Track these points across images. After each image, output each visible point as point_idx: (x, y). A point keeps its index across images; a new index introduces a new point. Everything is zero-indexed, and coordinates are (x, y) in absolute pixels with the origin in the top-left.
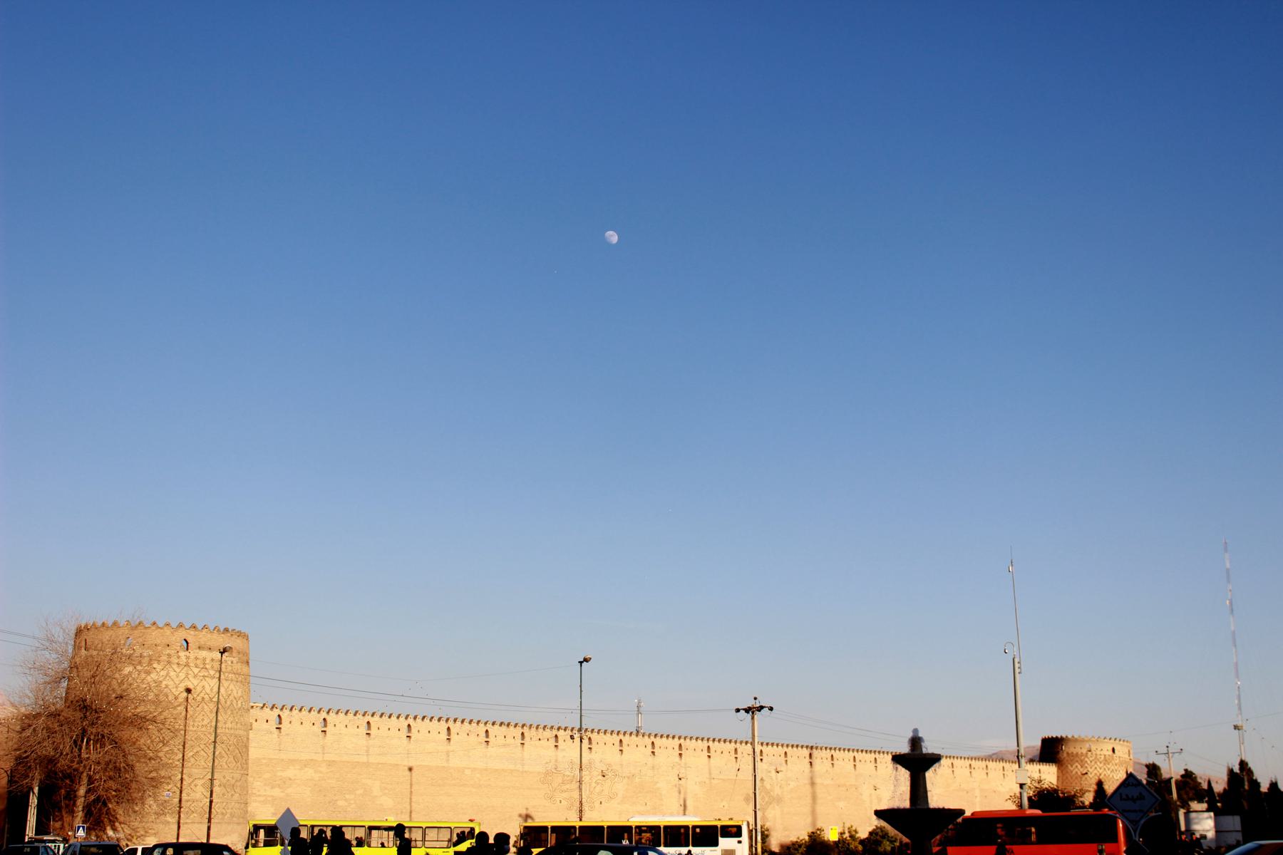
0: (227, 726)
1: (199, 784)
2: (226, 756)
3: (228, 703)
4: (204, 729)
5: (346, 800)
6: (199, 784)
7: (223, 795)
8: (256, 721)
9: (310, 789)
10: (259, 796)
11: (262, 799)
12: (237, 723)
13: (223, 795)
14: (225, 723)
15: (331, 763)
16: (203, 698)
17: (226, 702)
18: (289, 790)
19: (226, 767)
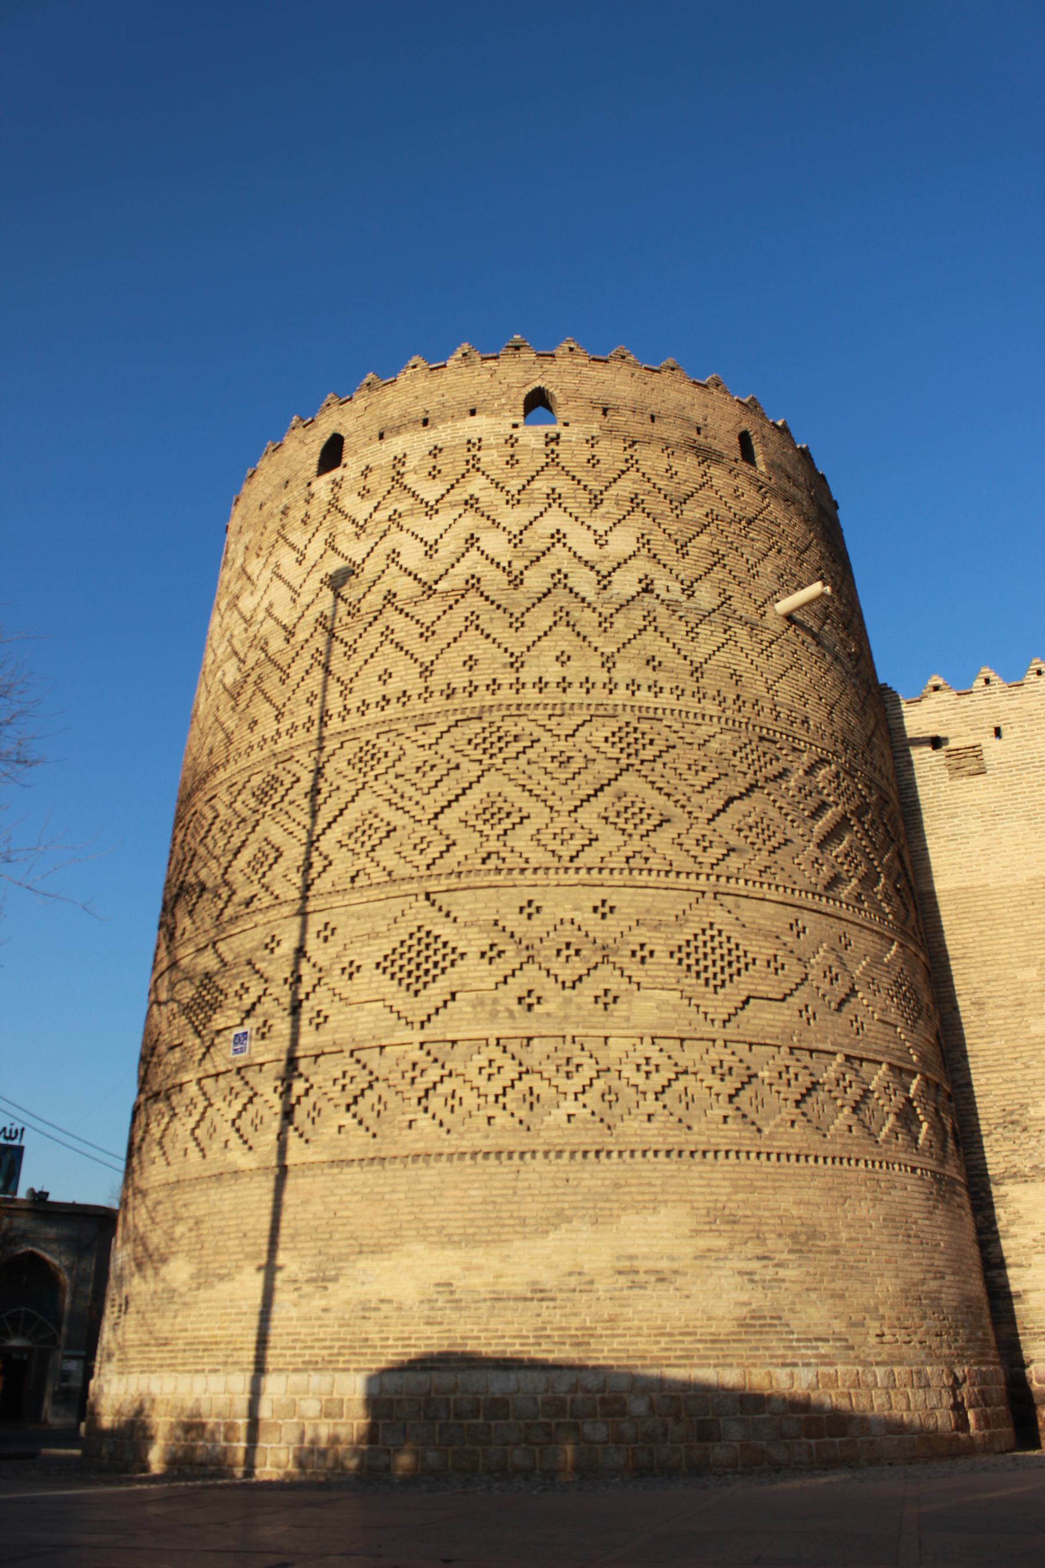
0: (528, 675)
2: (530, 805)
3: (536, 580)
6: (368, 964)
7: (528, 1001)
8: (998, 733)
12: (608, 662)
13: (528, 1001)
14: (516, 663)
16: (390, 597)
17: (517, 582)
19: (538, 857)
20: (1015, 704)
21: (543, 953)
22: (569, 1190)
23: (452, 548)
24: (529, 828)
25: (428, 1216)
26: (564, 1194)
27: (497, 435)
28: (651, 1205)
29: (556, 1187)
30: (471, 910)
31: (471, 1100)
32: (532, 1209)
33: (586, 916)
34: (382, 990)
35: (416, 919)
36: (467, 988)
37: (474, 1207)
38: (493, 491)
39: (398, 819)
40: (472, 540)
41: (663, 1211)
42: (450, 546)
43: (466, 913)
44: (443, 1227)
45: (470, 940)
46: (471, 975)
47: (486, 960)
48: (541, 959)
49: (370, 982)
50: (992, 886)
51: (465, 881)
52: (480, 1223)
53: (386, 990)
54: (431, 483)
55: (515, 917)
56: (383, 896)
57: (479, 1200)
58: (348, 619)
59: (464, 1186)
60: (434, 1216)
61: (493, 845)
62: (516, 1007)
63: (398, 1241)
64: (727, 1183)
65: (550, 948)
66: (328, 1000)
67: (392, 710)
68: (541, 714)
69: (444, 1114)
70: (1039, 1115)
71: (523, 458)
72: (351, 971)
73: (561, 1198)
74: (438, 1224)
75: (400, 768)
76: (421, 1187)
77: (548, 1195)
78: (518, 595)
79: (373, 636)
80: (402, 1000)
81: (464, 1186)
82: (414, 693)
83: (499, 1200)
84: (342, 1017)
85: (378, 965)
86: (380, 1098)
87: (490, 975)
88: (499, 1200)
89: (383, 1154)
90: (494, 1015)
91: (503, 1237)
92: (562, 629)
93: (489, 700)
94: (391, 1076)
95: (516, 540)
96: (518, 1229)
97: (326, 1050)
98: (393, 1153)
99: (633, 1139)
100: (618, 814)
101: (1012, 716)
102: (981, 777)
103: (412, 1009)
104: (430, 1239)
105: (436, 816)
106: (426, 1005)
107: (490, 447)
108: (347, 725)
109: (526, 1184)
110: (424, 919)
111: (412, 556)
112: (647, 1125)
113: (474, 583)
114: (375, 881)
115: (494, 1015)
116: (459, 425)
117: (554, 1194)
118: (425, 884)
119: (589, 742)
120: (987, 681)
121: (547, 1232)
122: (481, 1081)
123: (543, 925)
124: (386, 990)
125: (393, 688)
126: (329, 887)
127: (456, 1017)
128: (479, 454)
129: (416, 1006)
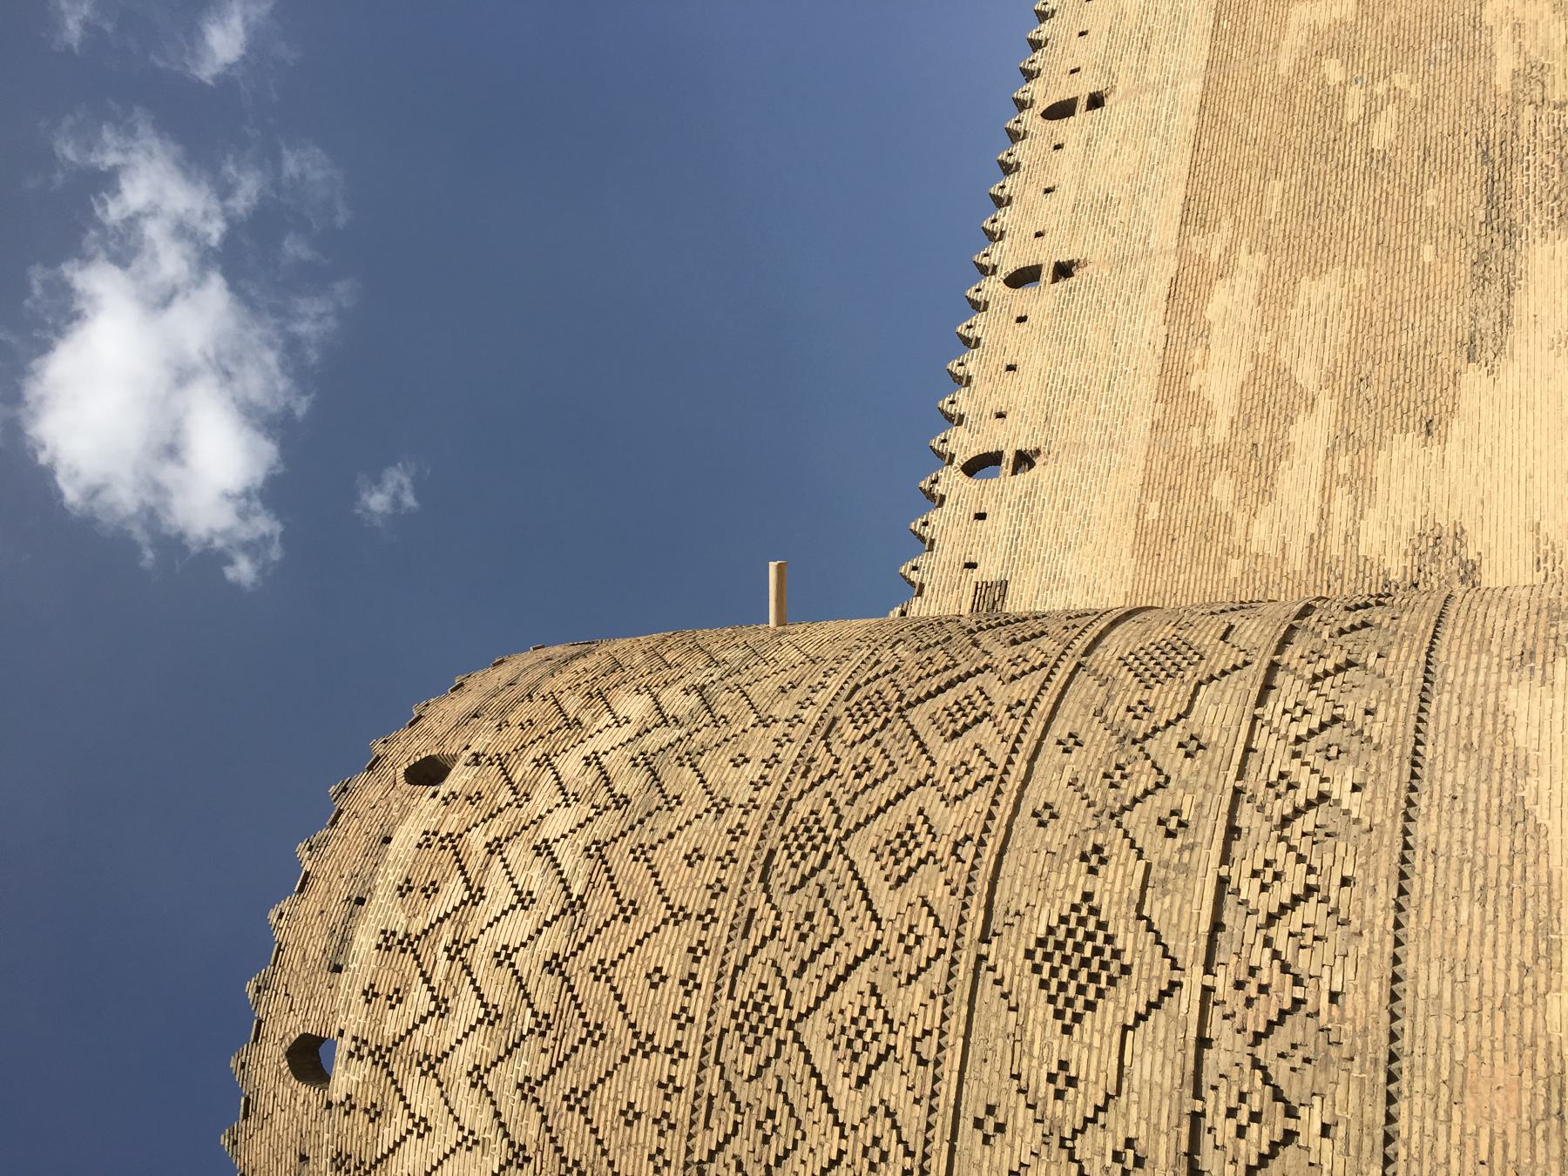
1: (1059, 1046)
4: (705, 973)
5: (1370, 115)
6: (1059, 1046)
9: (1305, 281)
10: (1324, 516)
11: (1341, 503)
14: (720, 807)
15: (1193, 217)
16: (553, 964)
17: (621, 802)
18: (1307, 375)
19: (980, 800)
20: (948, 547)
21: (1110, 801)
22: (1471, 796)
23: (536, 872)
24: (937, 811)
25: (1501, 989)
26: (1476, 802)
27: (432, 814)
28: (1501, 718)
29: (1464, 811)
30: (1023, 885)
31: (1309, 911)
32: (1499, 840)
33: (1072, 760)
34: (1107, 1030)
35: (1013, 961)
36: (1136, 897)
37: (1490, 915)
38: (497, 821)
39: (860, 979)
40: (543, 849)
41: (1510, 708)
42: (535, 877)
43: (1026, 890)
44: (1522, 965)
45: (1066, 886)
46: (1117, 888)
47: (1102, 869)
48: (1118, 805)
49: (1090, 1047)
50: (1129, 589)
51: (981, 886)
52: (1517, 909)
53: (1109, 1019)
54: (440, 897)
55: (1049, 833)
56: (964, 1010)
57: (1477, 909)
58: (551, 1034)
59: (1451, 926)
60: (1501, 978)
61: (943, 849)
62: (1179, 841)
63: (1542, 1043)
64: (1474, 658)
65: (1105, 795)
66: (1100, 1135)
67: (705, 973)
68: (796, 786)
69: (1326, 951)
70: (1401, 572)
71: (482, 785)
72: (1065, 1079)
73: (1482, 806)
74: (1514, 974)
75: (789, 968)
76: (1447, 996)
77: (1476, 822)
78: (636, 801)
79: (593, 993)
80: (1129, 998)
81: (1451, 926)
82: (699, 934)
83: (1479, 882)
84: (1134, 1109)
85: (1067, 1030)
86: (1282, 1055)
87: (1125, 865)
88: (1479, 882)
89: (1383, 1056)
90: (1185, 869)
91: (1545, 880)
92: (702, 762)
93: (751, 840)
94: (1250, 1028)
95: (568, 797)
96: (1530, 860)
97: (1184, 1147)
98: (1384, 1038)
99: (1400, 729)
100: (954, 721)
101: (958, 550)
102: (1010, 586)
103: (1149, 980)
104: (1542, 988)
105: (875, 918)
106: (1147, 959)
107: (441, 823)
108: (694, 1049)
109: (1456, 847)
110: (1016, 947)
111: (517, 927)
112: (1380, 716)
113: (597, 851)
114: (937, 1024)
115: (1185, 869)
116: (390, 858)
117: (1475, 813)
118: (967, 940)
119: (853, 744)
120: (915, 568)
121: (1537, 826)
122: (1282, 893)
123: (1071, 805)
124: (1109, 1019)
125: (675, 967)
126: (920, 1111)
127: (1175, 920)
128: (443, 833)
129: (1145, 974)
